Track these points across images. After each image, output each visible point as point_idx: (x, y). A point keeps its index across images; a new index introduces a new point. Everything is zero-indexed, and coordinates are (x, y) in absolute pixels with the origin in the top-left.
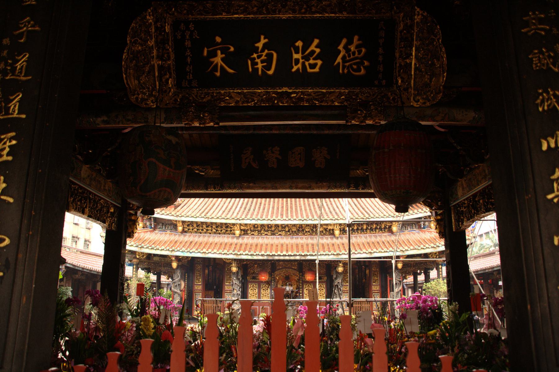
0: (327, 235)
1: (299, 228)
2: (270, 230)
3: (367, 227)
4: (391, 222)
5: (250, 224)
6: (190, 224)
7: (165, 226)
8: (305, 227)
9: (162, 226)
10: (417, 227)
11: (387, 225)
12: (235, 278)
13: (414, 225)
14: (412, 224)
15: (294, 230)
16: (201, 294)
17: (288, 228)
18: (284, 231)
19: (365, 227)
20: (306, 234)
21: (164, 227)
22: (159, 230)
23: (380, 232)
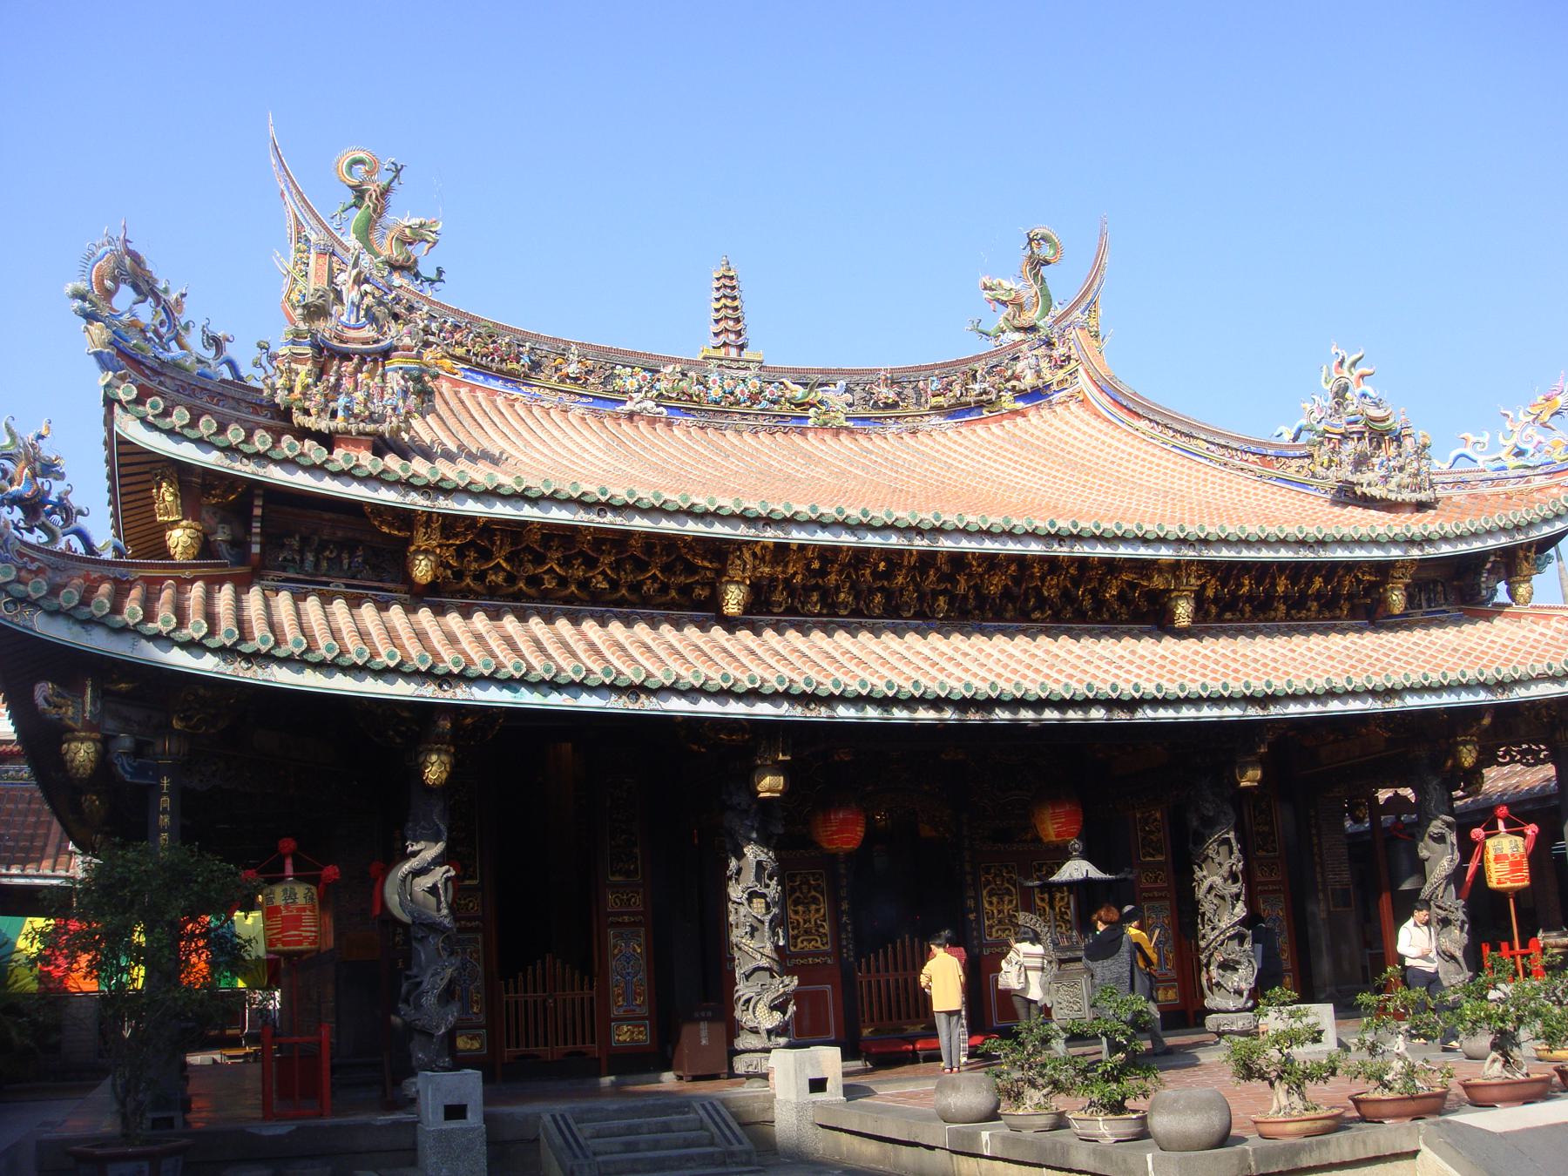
0: (1121, 622)
1: (1017, 581)
2: (882, 589)
3: (1286, 587)
4: (1384, 569)
5: (802, 547)
6: (471, 544)
7: (318, 553)
8: (1043, 579)
9: (301, 552)
10: (1452, 598)
11: (1359, 581)
12: (754, 835)
13: (1440, 588)
14: (1435, 582)
15: (995, 585)
16: (480, 937)
17: (966, 580)
18: (943, 592)
19: (1280, 589)
20: (1037, 615)
21: (310, 557)
22: (284, 575)
23: (1327, 615)
